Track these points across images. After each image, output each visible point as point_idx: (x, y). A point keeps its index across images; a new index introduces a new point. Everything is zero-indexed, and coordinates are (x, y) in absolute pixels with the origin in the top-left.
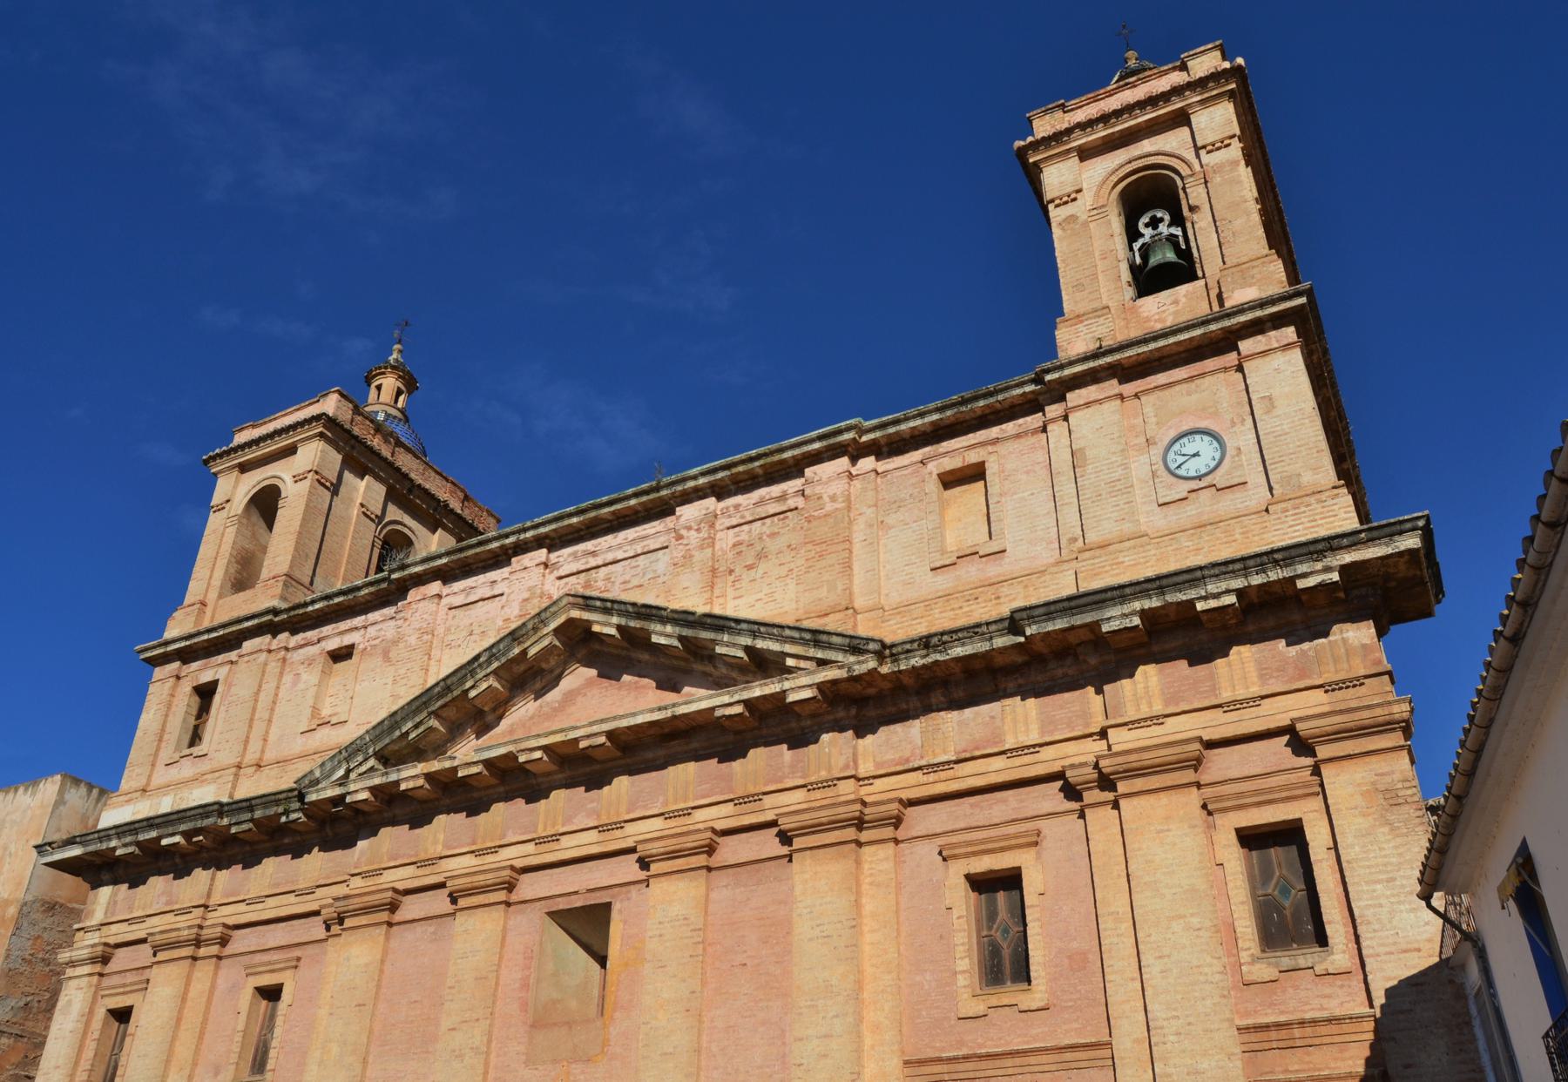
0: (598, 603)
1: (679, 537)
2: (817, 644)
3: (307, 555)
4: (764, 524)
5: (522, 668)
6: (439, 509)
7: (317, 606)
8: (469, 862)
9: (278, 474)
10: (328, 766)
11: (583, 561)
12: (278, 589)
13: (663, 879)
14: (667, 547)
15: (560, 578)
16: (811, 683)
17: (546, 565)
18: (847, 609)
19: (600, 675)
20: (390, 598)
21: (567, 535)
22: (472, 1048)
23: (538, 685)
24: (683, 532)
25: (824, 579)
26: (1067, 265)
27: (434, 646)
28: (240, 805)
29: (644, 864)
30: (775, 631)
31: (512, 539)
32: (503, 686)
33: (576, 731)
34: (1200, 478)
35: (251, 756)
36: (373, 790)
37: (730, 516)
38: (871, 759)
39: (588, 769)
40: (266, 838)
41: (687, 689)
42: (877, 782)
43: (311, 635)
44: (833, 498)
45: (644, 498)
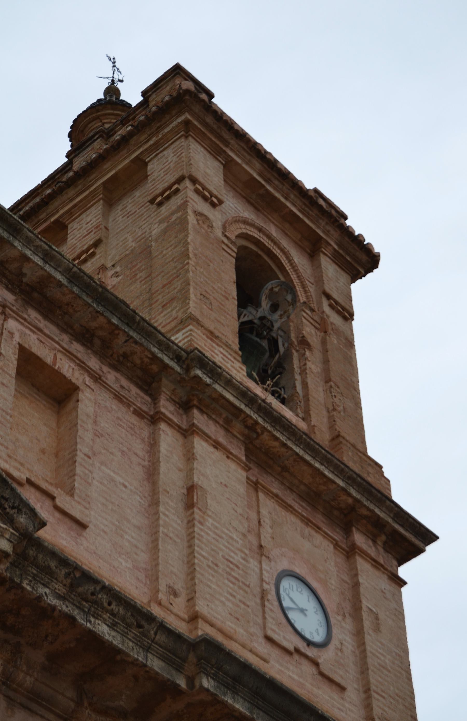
34: (309, 643)
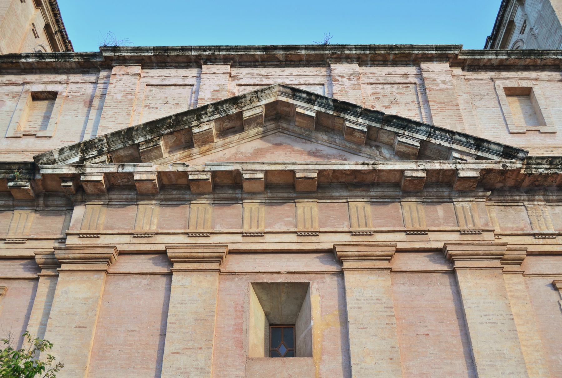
2: (478, 148)
4: (393, 87)
11: (259, 79)
13: (356, 272)
14: (323, 85)
15: (240, 85)
16: (477, 168)
22: (197, 368)
26: (559, 11)
33: (294, 166)
38: (497, 224)
44: (444, 82)
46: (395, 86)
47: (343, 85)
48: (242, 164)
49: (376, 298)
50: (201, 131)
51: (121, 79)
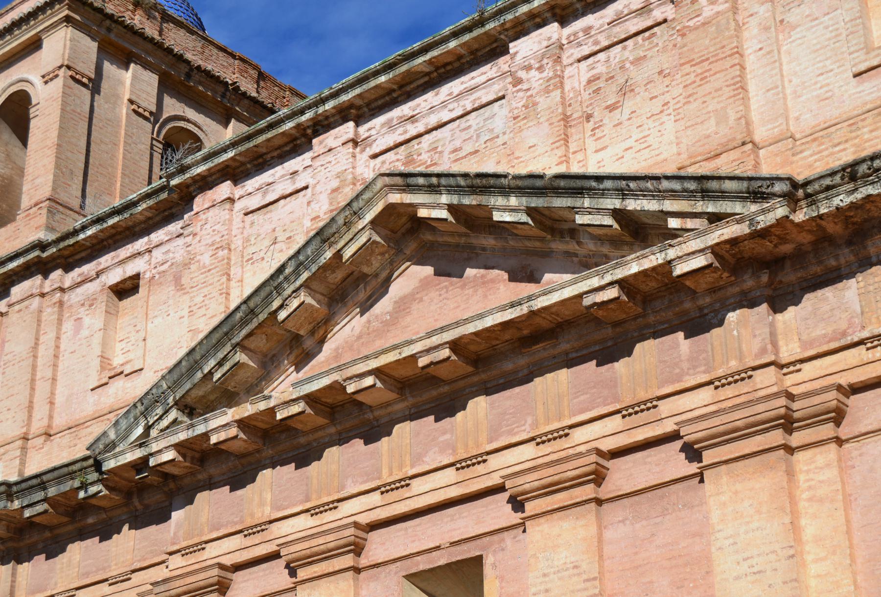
0: (421, 181)
1: (518, 82)
2: (706, 194)
3: (72, 172)
4: (624, 48)
5: (339, 275)
6: (228, 94)
7: (89, 232)
8: (304, 522)
9: (25, 76)
10: (124, 424)
11: (400, 131)
12: (42, 218)
13: (542, 520)
14: (503, 97)
15: (375, 156)
16: (702, 246)
17: (355, 142)
18: (744, 144)
19: (437, 273)
20: (174, 210)
21: (376, 100)
23: (362, 296)
24: (522, 74)
25: (710, 108)
27: (232, 263)
28: (30, 483)
29: (517, 504)
30: (649, 185)
31: (309, 115)
32: (318, 302)
33: (412, 347)
35: (38, 425)
36: (179, 447)
37: (580, 45)
38: (796, 338)
39: (434, 393)
40: (65, 519)
41: (548, 277)
42: (806, 366)
43: (88, 269)
45: (467, 37)
46: (630, 43)
47: (528, 89)
48: (339, 368)
49: (572, 565)
50: (289, 313)
51: (207, 219)
